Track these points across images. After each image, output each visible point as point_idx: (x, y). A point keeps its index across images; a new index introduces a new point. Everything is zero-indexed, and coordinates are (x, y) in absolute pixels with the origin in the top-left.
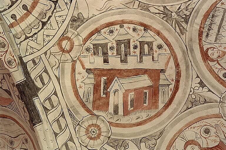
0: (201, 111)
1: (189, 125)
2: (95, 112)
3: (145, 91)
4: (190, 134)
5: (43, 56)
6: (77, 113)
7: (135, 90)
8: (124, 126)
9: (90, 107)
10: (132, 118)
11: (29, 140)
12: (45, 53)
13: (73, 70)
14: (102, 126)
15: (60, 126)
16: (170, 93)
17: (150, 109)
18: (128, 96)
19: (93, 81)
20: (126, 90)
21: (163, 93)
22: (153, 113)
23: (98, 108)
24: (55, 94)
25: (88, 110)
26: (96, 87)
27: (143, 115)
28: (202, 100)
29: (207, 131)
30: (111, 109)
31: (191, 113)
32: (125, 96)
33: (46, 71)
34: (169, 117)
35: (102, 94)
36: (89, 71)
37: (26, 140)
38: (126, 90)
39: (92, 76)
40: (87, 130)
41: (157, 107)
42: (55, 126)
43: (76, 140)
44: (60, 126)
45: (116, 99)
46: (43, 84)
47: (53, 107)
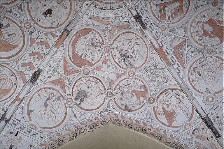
0: (200, 10)
1: (196, 17)
2: (162, 21)
3: (178, 8)
4: (197, 20)
5: (140, 3)
6: (156, 22)
7: (174, 9)
8: (173, 23)
9: (160, 19)
10: (175, 20)
11: (139, 38)
12: (140, 2)
13: (151, 6)
14: (165, 25)
15: (152, 29)
16: (187, 6)
17: (180, 15)
18: (172, 12)
19: (158, 9)
20: (171, 10)
21: (185, 7)
22: (182, 16)
23: (163, 19)
24: (147, 17)
25: (159, 21)
26: (160, 11)
27: (179, 18)
28: (200, 5)
29: (204, 16)
30: (167, 18)
31: (197, 12)
32: (171, 12)
33: (142, 9)
34: (188, 16)
35: (163, 13)
36: (156, 5)
37: (138, 39)
38: (171, 10)
39: (158, 7)
40: (161, 28)
41: (183, 13)
42: (150, 29)
43: (158, 32)
44: (152, 29)
45: (168, 14)
46: (142, 14)
47: (148, 22)
